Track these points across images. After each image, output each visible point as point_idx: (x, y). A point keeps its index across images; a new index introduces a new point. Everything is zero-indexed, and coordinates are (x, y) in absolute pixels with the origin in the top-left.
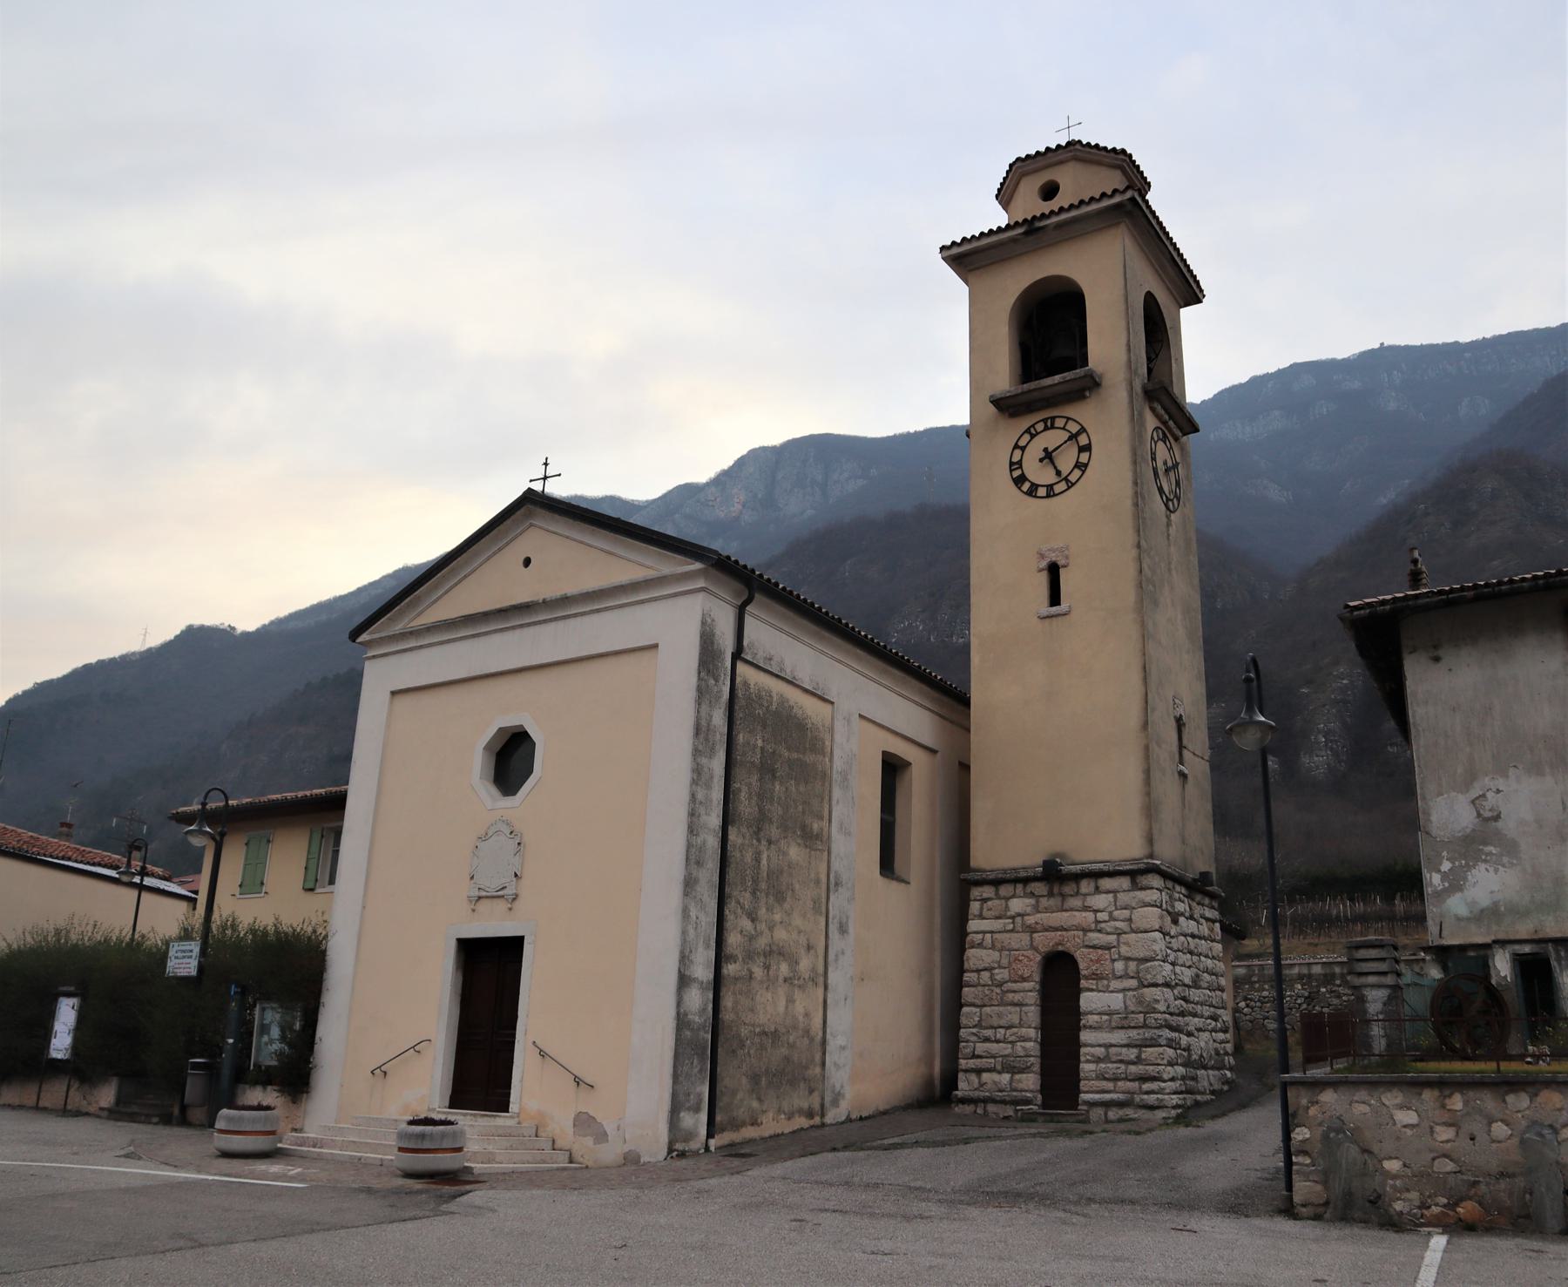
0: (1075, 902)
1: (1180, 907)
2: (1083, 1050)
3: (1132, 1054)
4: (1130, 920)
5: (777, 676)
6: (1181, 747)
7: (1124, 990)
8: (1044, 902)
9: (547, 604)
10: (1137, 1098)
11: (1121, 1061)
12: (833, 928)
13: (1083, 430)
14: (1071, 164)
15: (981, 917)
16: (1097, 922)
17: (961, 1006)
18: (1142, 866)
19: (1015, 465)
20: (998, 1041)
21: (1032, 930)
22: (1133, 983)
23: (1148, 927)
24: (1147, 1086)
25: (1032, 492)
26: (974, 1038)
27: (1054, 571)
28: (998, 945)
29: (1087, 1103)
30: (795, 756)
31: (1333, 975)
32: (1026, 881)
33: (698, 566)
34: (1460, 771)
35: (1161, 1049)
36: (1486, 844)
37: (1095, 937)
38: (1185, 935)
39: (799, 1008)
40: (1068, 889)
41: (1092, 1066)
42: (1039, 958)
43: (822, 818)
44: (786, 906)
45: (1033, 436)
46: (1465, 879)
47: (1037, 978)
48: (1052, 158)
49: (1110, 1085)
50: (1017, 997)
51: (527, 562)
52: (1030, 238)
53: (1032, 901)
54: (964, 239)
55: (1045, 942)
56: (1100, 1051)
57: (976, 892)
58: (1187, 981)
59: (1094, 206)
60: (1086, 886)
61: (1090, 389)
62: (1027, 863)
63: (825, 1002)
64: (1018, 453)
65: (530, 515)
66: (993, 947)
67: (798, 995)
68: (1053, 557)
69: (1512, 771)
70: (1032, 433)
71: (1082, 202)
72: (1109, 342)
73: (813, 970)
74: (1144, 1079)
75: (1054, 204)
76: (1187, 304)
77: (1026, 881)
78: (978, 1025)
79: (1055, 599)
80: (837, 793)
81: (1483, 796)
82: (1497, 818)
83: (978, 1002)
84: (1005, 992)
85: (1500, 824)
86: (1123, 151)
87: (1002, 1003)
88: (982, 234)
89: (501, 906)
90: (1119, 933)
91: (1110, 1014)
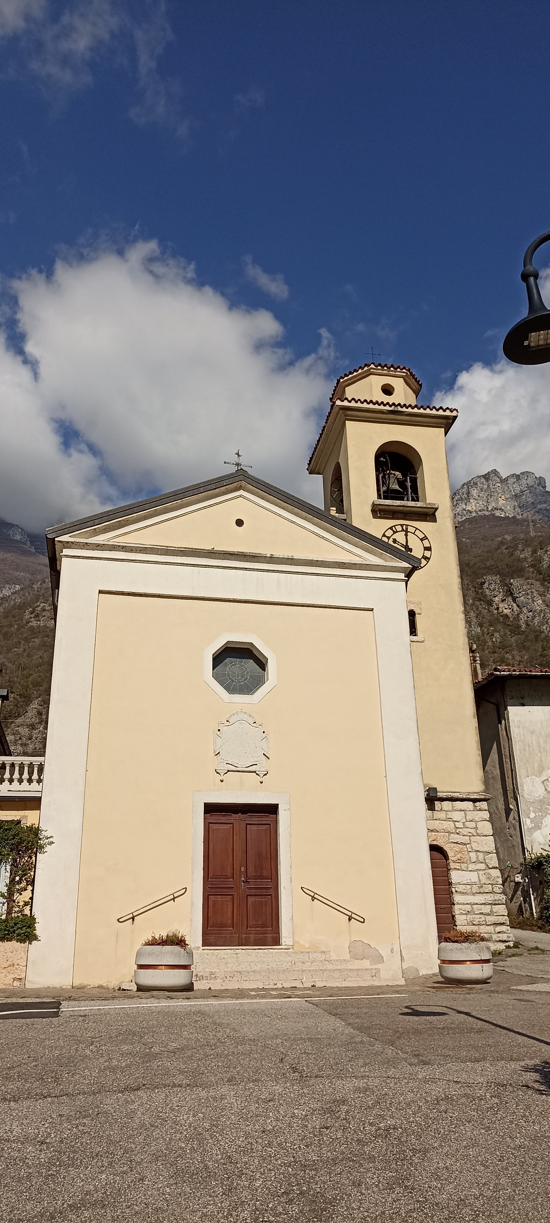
2: (456, 907)
3: (487, 909)
4: (476, 828)
9: (272, 560)
10: (495, 937)
11: (482, 913)
13: (425, 538)
18: (483, 797)
22: (483, 866)
23: (487, 834)
24: (499, 929)
27: (412, 614)
34: (536, 765)
37: (455, 838)
41: (464, 917)
56: (468, 908)
60: (446, 805)
75: (386, 399)
79: (413, 630)
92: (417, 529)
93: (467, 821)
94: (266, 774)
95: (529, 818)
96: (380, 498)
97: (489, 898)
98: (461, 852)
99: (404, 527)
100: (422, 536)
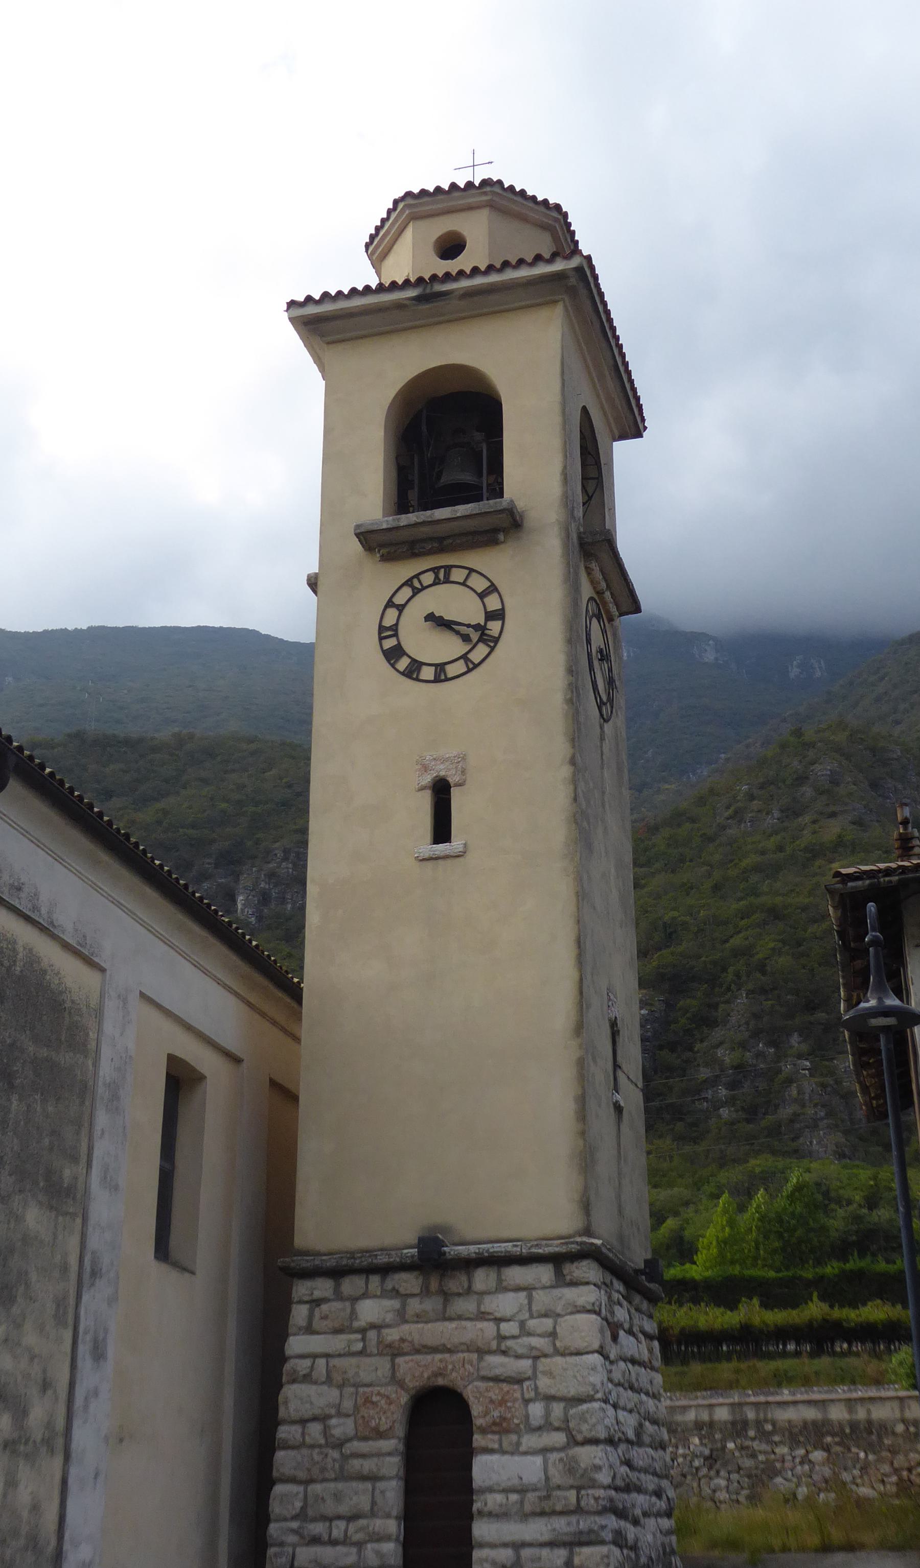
0: (466, 1305)
1: (621, 1314)
2: (477, 1554)
4: (553, 1334)
5: (27, 919)
6: (616, 1066)
7: (544, 1451)
8: (415, 1306)
12: (84, 1349)
13: (493, 589)
14: (485, 212)
15: (309, 1330)
16: (501, 1338)
17: (272, 1483)
18: (574, 1248)
19: (386, 631)
20: (333, 1543)
21: (394, 1351)
22: (559, 1438)
23: (581, 1345)
25: (413, 671)
26: (292, 1539)
27: (441, 792)
28: (337, 1378)
30: (44, 1052)
31: (745, 1423)
32: (385, 1270)
35: (604, 1549)
37: (496, 1363)
38: (625, 1360)
39: (24, 1495)
40: (455, 1283)
42: (404, 1398)
43: (75, 1159)
44: (15, 1310)
45: (416, 592)
47: (400, 1431)
48: (458, 200)
50: (368, 1466)
52: (425, 307)
53: (395, 1304)
54: (326, 295)
55: (416, 1371)
57: (301, 1289)
58: (631, 1434)
59: (524, 273)
60: (482, 1278)
61: (505, 531)
62: (389, 1240)
63: (64, 1482)
64: (392, 614)
66: (329, 1381)
67: (24, 1472)
68: (442, 770)
70: (414, 586)
71: (506, 264)
72: (532, 467)
73: (49, 1425)
75: (453, 266)
76: (623, 437)
77: (385, 1270)
78: (302, 1516)
79: (442, 830)
80: (102, 1119)
83: (302, 1475)
84: (345, 1458)
86: (558, 207)
87: (343, 1476)
88: (354, 291)
90: (536, 1356)
91: (522, 1490)
92: (471, 570)
93: (532, 1317)
97: (561, 1525)
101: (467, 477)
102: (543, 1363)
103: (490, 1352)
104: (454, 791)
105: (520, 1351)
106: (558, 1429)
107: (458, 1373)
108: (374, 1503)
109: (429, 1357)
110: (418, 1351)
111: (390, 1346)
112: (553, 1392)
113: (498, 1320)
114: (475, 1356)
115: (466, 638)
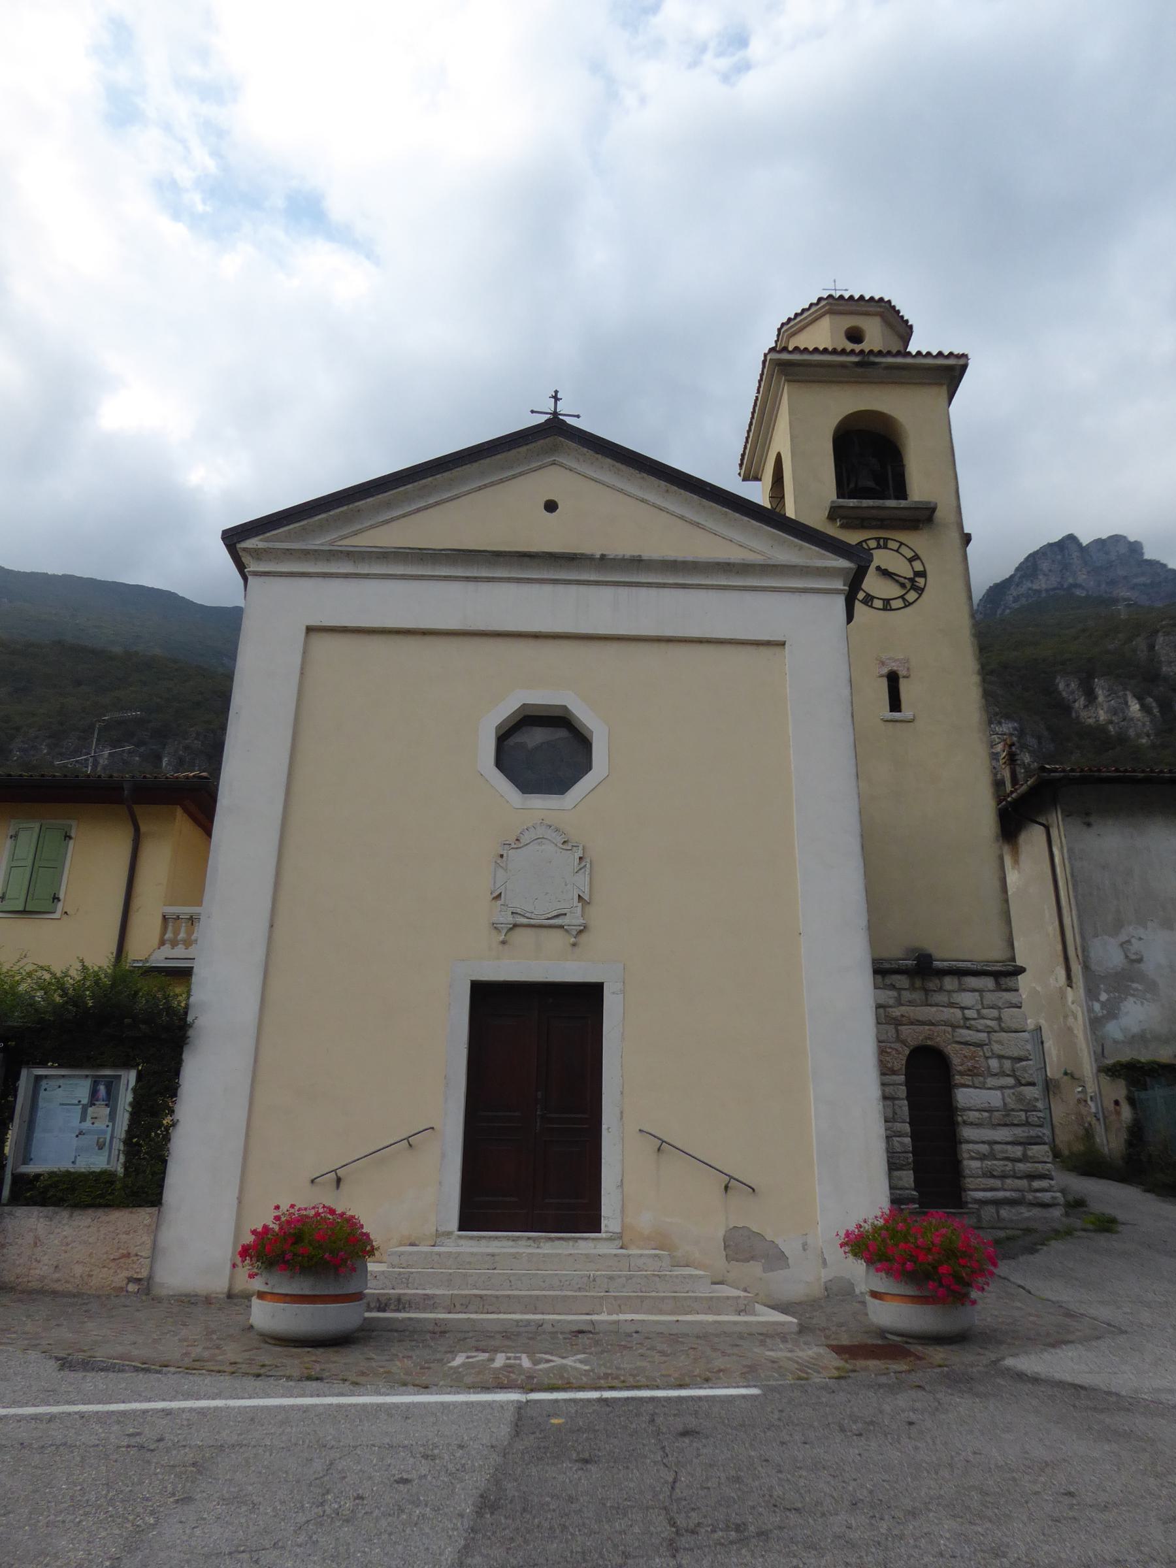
0: (942, 998)
3: (1018, 1151)
4: (999, 1019)
7: (1001, 1088)
8: (906, 995)
9: (603, 562)
10: (1029, 1196)
11: (1007, 1159)
13: (916, 557)
16: (966, 1019)
22: (1010, 1081)
24: (1036, 1184)
27: (893, 680)
29: (977, 1201)
33: (843, 563)
36: (1133, 982)
40: (932, 984)
41: (975, 1164)
42: (907, 1052)
46: (1119, 1009)
49: (997, 1183)
51: (551, 506)
52: (860, 370)
53: (894, 993)
55: (914, 1035)
56: (984, 1148)
60: (949, 983)
65: (554, 449)
68: (894, 666)
69: (1149, 923)
74: (1032, 1177)
79: (895, 704)
81: (1129, 942)
82: (1140, 961)
85: (1142, 966)
86: (911, 327)
89: (556, 941)
90: (990, 1031)
92: (902, 544)
94: (581, 932)
95: (1098, 1000)
96: (843, 497)
97: (1019, 1132)
98: (973, 1058)
99: (882, 542)
100: (910, 554)
101: (871, 484)
102: (995, 1036)
103: (959, 1027)
104: (901, 680)
105: (980, 1028)
106: (1008, 1075)
107: (942, 1038)
108: (895, 1113)
109: (921, 1028)
110: (912, 1024)
111: (894, 1019)
112: (1002, 1053)
113: (963, 1008)
114: (949, 1029)
115: (903, 586)
